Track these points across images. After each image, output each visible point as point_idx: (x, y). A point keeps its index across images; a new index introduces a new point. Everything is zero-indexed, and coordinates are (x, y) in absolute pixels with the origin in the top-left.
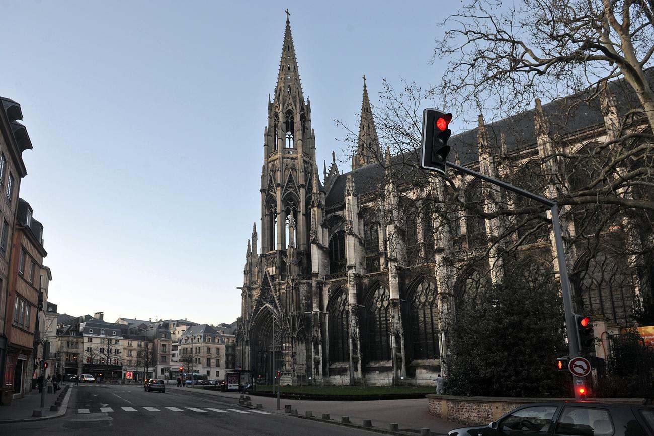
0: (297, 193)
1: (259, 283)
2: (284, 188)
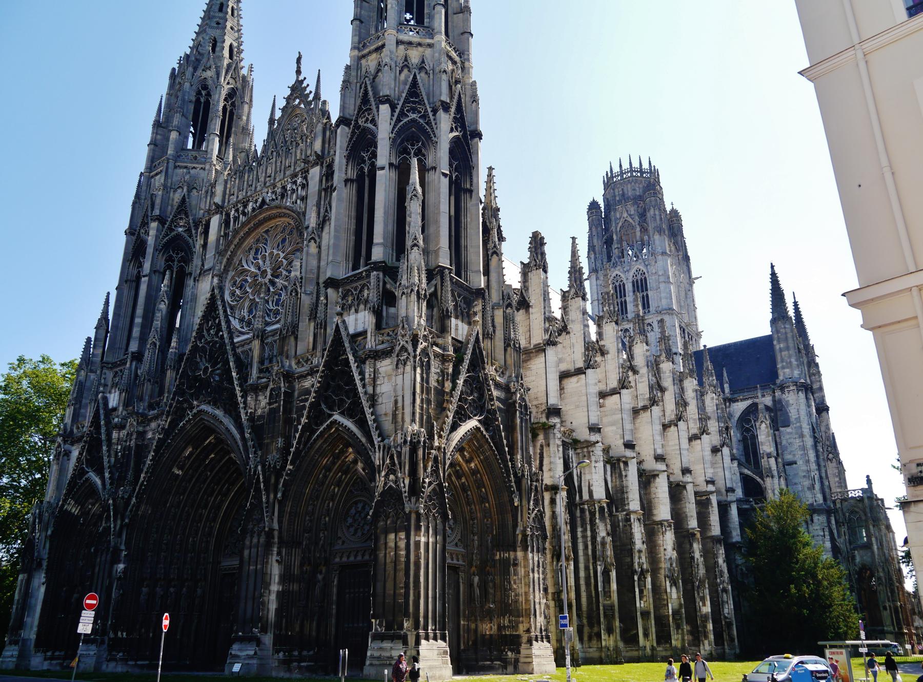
0: (429, 123)
1: (319, 361)
2: (397, 111)
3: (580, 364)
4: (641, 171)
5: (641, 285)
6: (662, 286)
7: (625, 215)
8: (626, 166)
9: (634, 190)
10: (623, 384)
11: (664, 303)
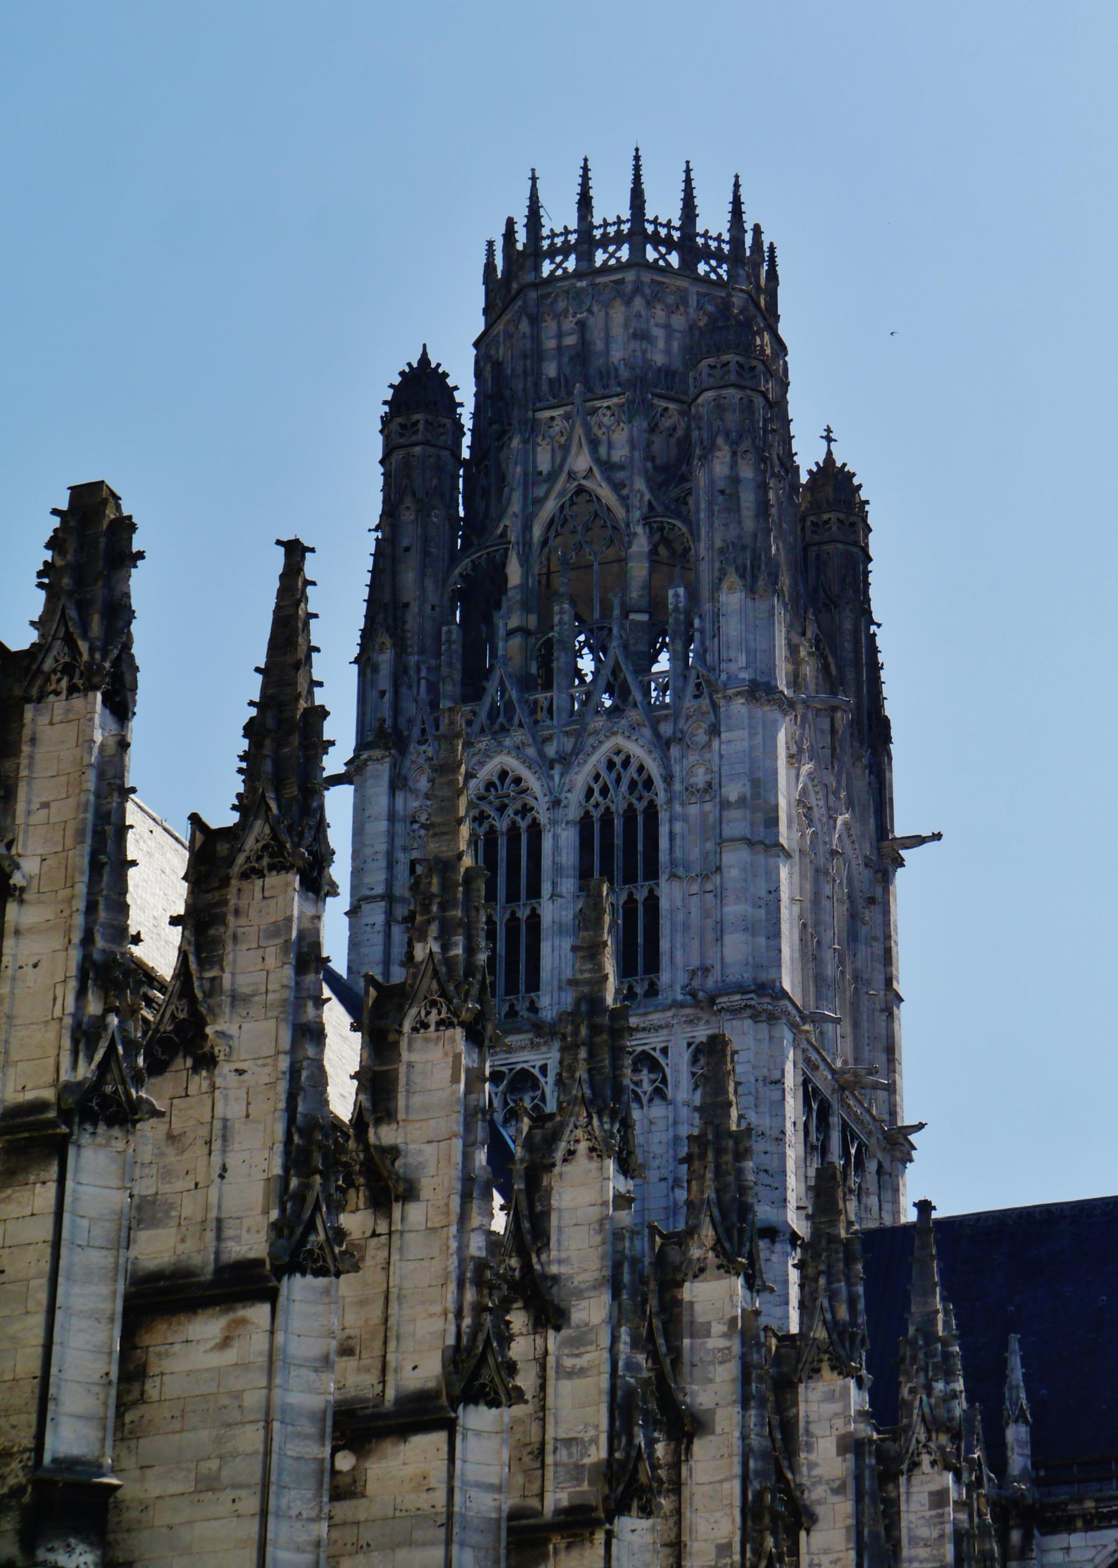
3: (251, 1242)
4: (687, 240)
5: (624, 846)
6: (734, 859)
7: (581, 462)
8: (611, 206)
9: (642, 336)
10: (476, 1374)
11: (736, 950)
